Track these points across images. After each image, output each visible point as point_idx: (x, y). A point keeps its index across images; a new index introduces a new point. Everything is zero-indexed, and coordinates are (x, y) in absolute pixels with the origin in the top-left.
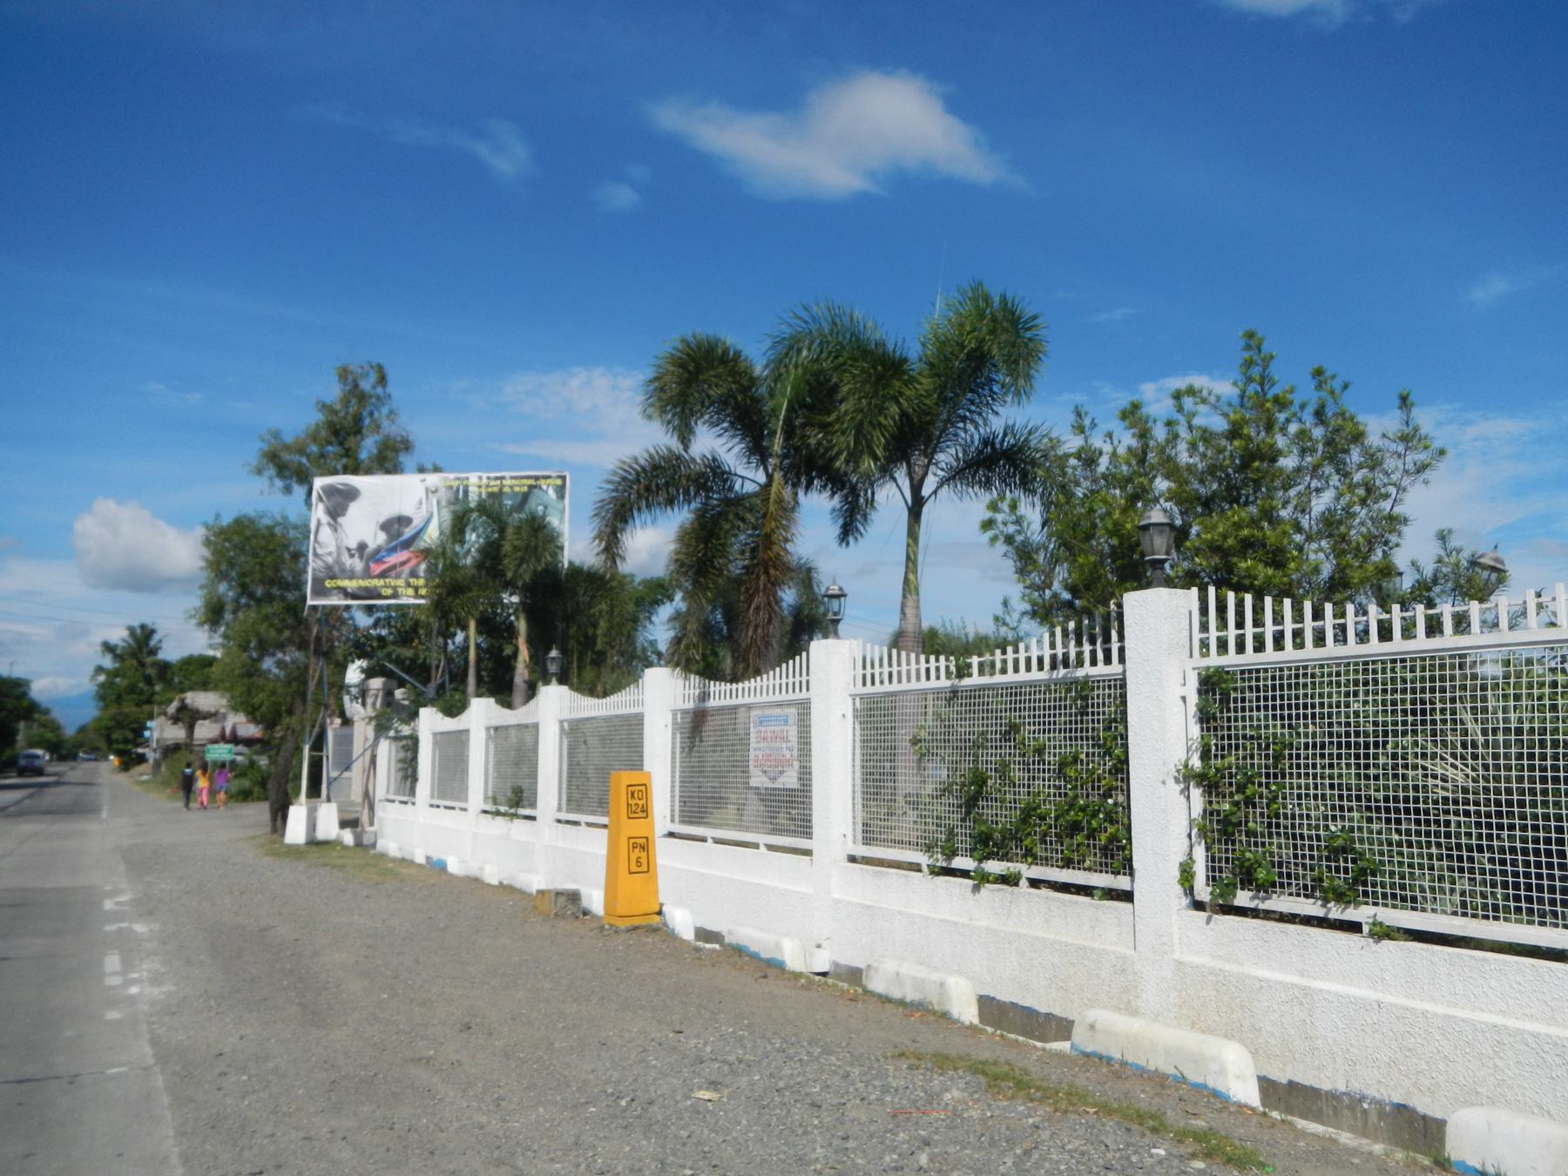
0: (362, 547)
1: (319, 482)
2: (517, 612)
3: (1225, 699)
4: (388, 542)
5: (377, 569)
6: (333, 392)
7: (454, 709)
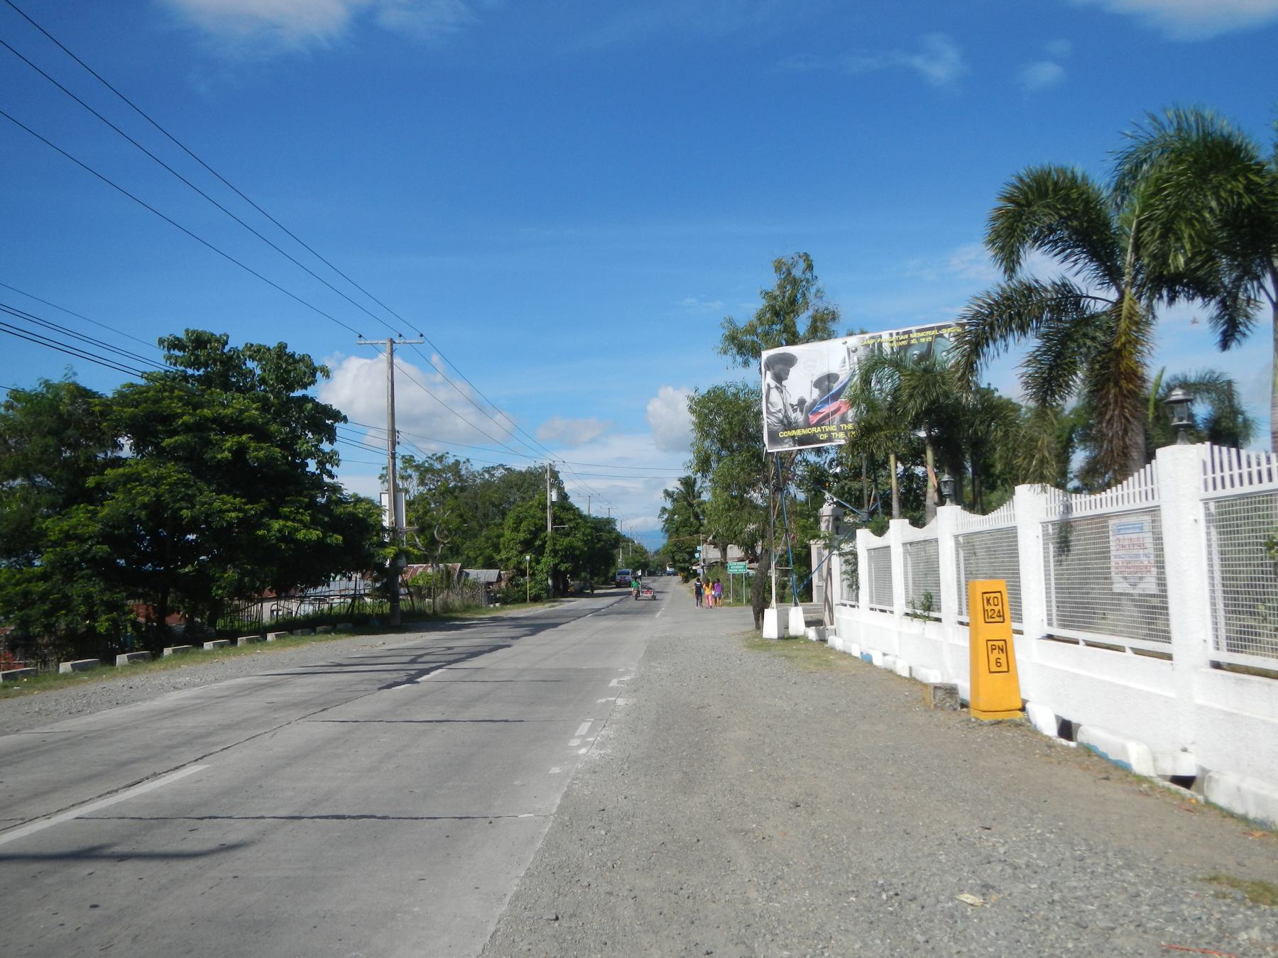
0: (802, 402)
1: (766, 354)
2: (938, 441)
4: (821, 397)
5: (814, 419)
6: (772, 282)
7: (880, 530)
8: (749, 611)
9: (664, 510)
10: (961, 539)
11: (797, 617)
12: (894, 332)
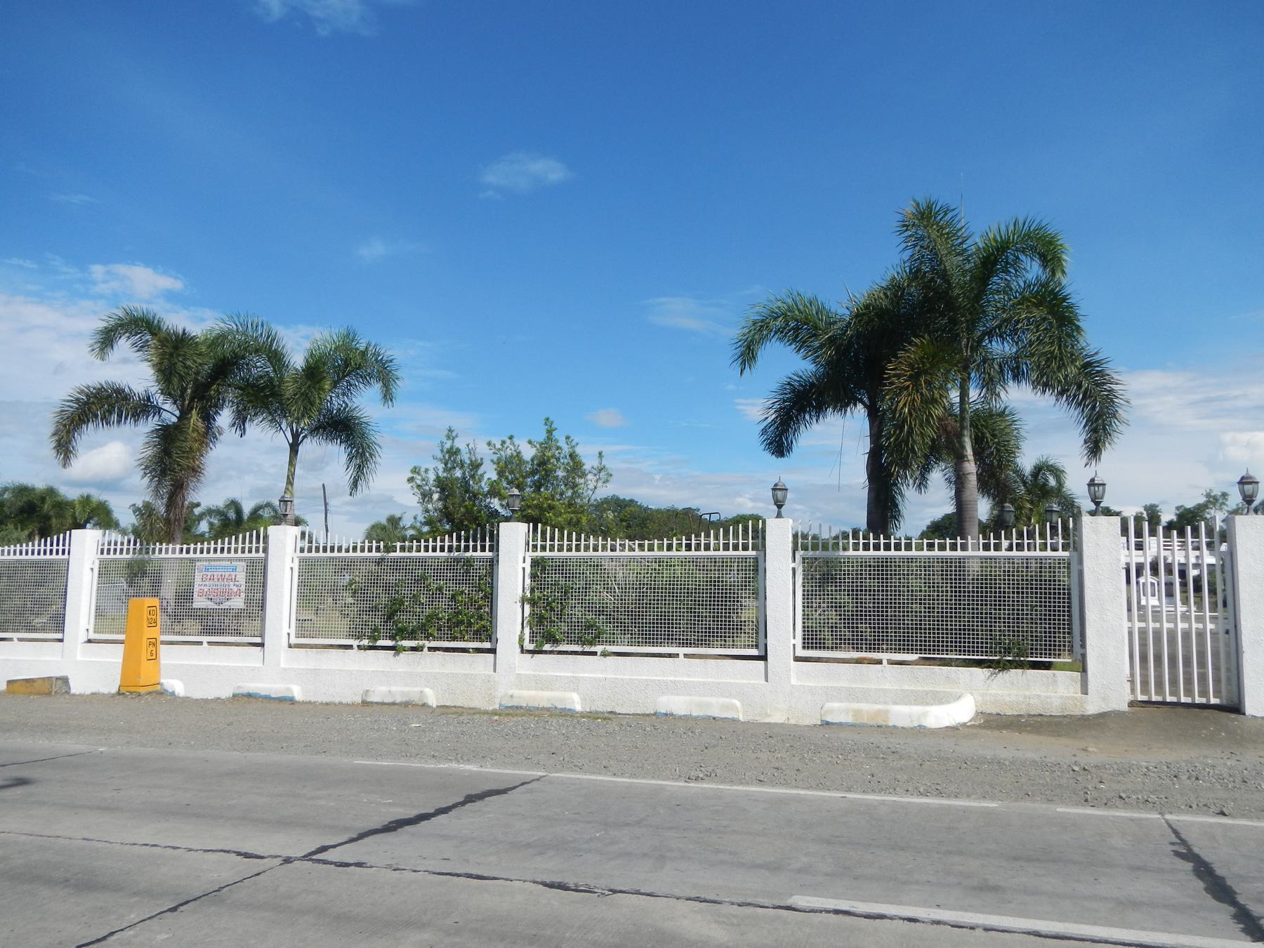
3: (544, 569)
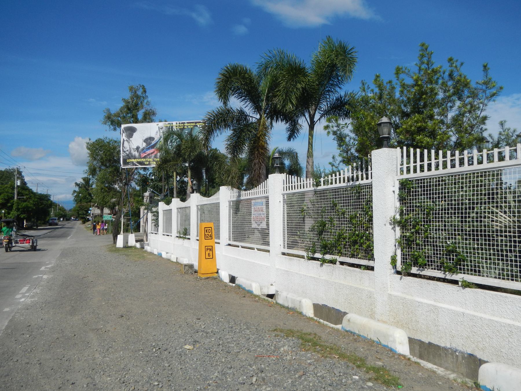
0: (138, 148)
1: (123, 126)
3: (409, 192)
5: (143, 155)
6: (128, 95)
7: (168, 203)
8: (111, 236)
9: (75, 191)
10: (199, 207)
11: (132, 238)
12: (178, 122)
